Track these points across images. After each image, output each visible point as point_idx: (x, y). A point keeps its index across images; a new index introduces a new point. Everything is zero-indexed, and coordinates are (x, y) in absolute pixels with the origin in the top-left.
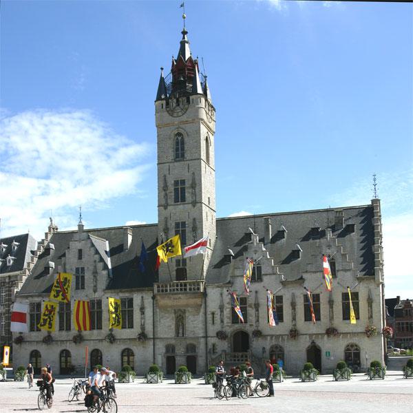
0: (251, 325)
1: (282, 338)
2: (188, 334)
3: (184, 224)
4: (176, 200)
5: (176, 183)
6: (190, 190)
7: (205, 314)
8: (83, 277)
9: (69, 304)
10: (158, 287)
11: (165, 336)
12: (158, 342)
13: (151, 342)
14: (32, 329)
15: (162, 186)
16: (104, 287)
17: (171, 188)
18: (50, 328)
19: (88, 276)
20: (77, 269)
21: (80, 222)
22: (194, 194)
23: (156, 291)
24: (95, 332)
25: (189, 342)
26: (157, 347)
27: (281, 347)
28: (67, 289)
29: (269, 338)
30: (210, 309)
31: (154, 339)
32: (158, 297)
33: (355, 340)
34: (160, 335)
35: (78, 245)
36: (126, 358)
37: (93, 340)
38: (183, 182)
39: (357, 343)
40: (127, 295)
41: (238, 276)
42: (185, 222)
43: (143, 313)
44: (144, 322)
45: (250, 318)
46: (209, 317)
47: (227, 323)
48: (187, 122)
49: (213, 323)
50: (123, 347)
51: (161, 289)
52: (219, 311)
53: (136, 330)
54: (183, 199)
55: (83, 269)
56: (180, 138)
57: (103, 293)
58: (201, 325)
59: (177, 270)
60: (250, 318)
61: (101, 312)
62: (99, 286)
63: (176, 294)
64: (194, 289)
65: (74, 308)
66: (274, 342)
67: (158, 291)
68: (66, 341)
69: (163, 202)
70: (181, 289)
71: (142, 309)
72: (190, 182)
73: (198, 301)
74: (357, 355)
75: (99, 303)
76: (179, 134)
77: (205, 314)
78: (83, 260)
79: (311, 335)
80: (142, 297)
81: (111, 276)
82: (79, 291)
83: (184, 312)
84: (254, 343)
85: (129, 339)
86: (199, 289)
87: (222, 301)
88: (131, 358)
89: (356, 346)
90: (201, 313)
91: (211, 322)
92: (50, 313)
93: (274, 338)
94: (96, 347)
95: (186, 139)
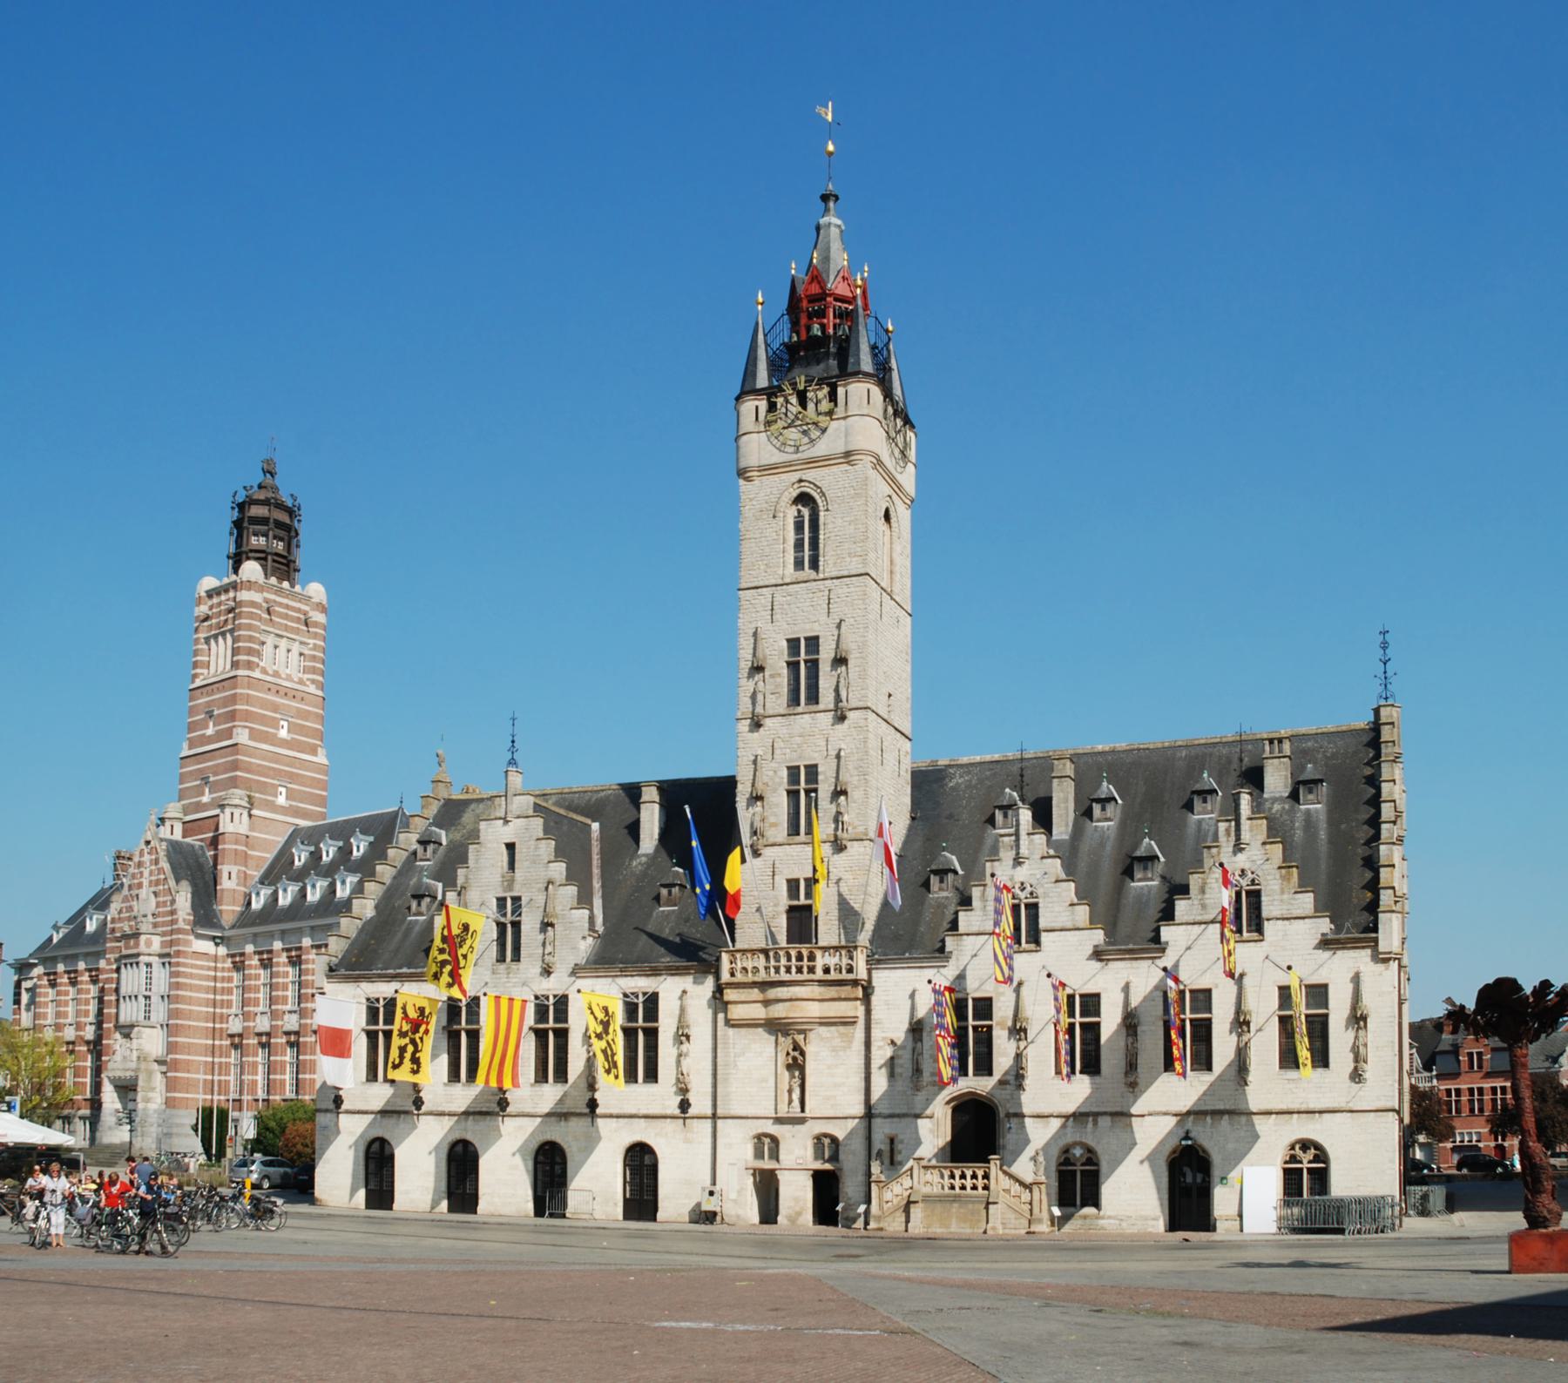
8: (516, 925)
13: (708, 1124)
18: (415, 1072)
19: (529, 924)
20: (501, 902)
28: (465, 957)
32: (730, 995)
40: (640, 984)
41: (968, 935)
42: (816, 766)
43: (682, 1036)
51: (739, 965)
55: (517, 900)
59: (792, 910)
70: (799, 970)
74: (1321, 1178)
75: (562, 1002)
78: (519, 873)
80: (684, 992)
81: (600, 927)
82: (502, 967)
84: (1009, 1136)
85: (646, 1117)
86: (850, 970)
89: (1318, 1147)
92: (415, 1029)
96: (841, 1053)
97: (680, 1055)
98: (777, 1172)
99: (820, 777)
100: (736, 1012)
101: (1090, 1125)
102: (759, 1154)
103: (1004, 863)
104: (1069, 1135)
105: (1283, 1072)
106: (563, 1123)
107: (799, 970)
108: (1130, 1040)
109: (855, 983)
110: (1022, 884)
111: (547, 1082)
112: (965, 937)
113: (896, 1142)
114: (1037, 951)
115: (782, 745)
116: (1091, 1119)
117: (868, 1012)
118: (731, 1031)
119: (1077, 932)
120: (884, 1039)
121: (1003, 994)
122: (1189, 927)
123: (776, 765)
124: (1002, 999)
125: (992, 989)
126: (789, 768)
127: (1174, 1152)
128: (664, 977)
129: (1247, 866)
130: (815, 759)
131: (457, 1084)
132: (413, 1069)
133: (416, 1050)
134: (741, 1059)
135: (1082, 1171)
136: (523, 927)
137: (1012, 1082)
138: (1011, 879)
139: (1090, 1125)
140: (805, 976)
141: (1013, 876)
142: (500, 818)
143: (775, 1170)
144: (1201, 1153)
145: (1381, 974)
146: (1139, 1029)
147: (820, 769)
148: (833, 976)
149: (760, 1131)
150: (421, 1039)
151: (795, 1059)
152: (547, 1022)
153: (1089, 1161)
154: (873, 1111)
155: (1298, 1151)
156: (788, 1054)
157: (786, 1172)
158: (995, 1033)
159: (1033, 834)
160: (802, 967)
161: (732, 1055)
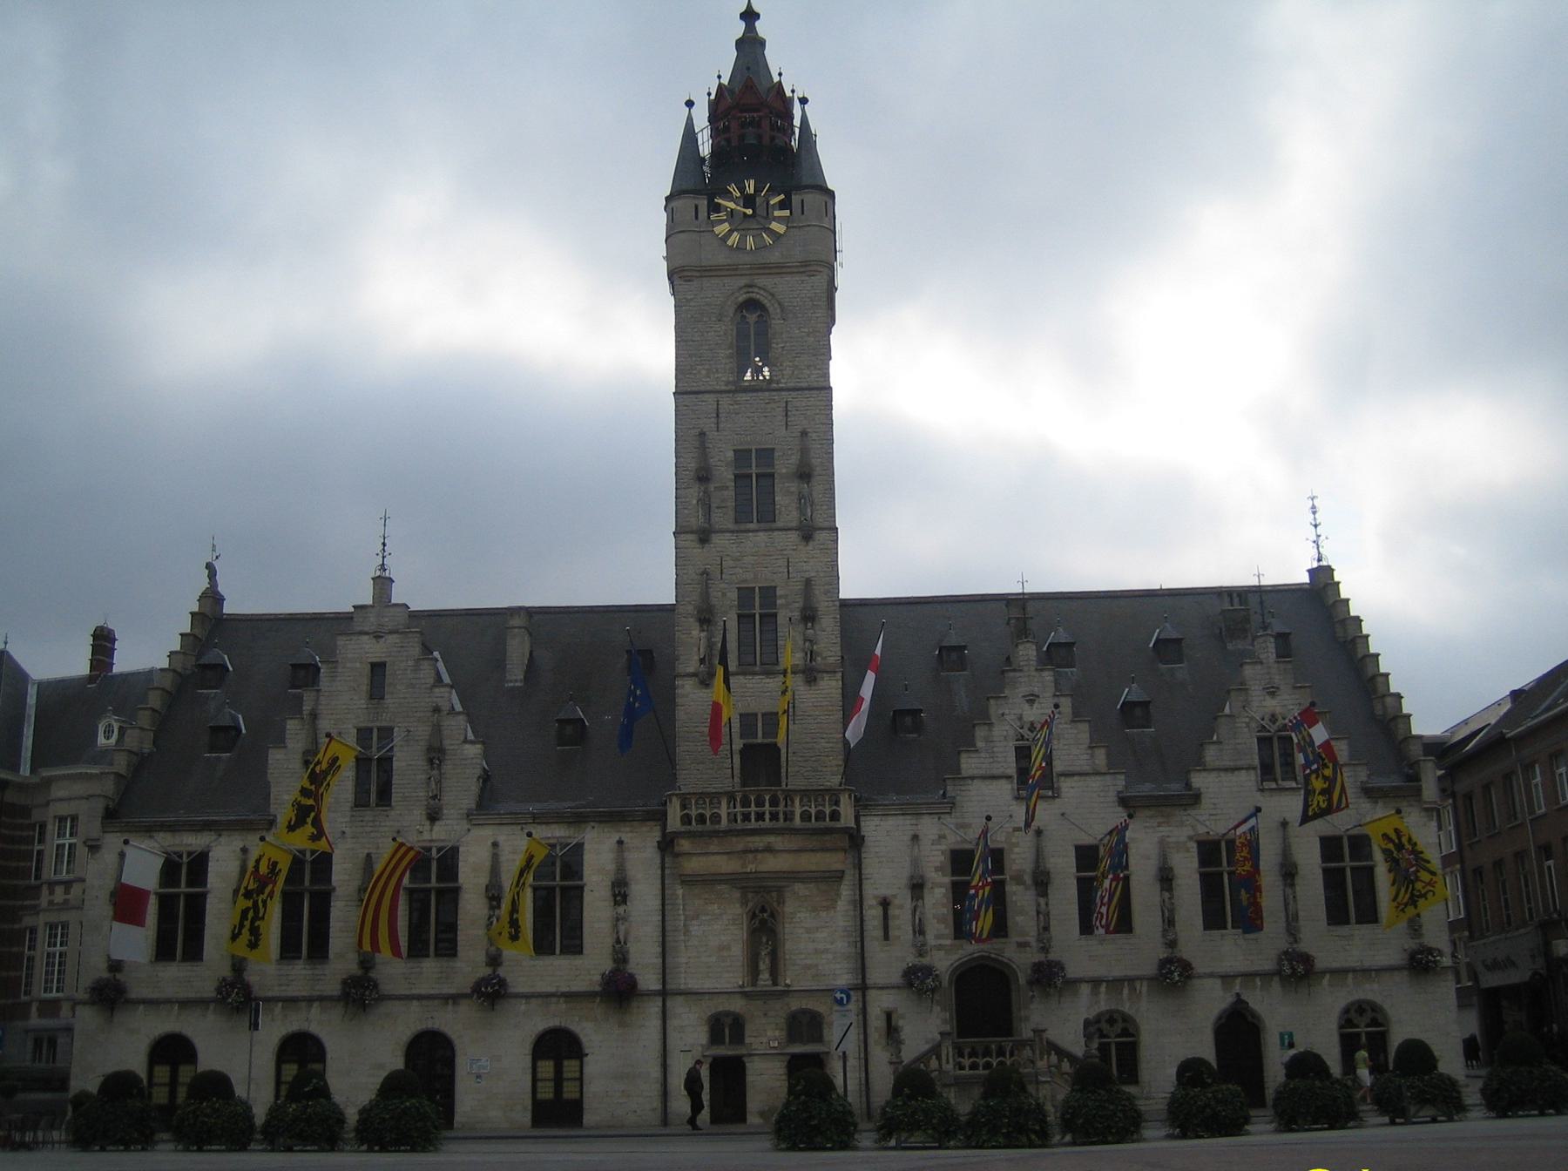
0: (1023, 945)
1: (1133, 989)
2: (792, 978)
3: (769, 593)
4: (742, 515)
5: (742, 456)
6: (794, 486)
7: (859, 903)
8: (386, 763)
9: (323, 863)
10: (684, 807)
11: (708, 985)
12: (677, 1006)
13: (654, 1007)
14: (164, 951)
15: (693, 465)
16: (469, 801)
17: (725, 474)
19: (407, 762)
20: (364, 734)
21: (383, 567)
22: (804, 501)
23: (674, 821)
24: (430, 966)
25: (795, 1004)
26: (673, 1023)
27: (1126, 1019)
29: (1085, 989)
30: (872, 892)
31: (664, 994)
32: (685, 845)
33: (1370, 991)
34: (687, 979)
35: (374, 650)
36: (546, 1068)
37: (420, 998)
38: (766, 455)
39: (1378, 1000)
40: (558, 832)
41: (972, 778)
44: (627, 934)
45: (1019, 919)
46: (873, 914)
47: (938, 937)
48: (779, 269)
49: (886, 937)
50: (541, 1023)
51: (694, 813)
52: (907, 894)
53: (591, 966)
54: (767, 516)
55: (386, 733)
56: (752, 318)
57: (465, 825)
58: (842, 946)
59: (747, 751)
60: (1019, 919)
61: (456, 891)
62: (447, 798)
63: (754, 832)
64: (820, 816)
65: (343, 875)
66: (1104, 1004)
67: (686, 820)
68: (310, 1000)
69: (697, 521)
70: (760, 817)
71: (620, 892)
72: (794, 459)
73: (834, 861)
75: (449, 861)
76: (751, 305)
77: (859, 903)
79: (1227, 979)
80: (620, 842)
82: (368, 815)
83: (781, 901)
86: (835, 816)
87: (915, 862)
88: (570, 1066)
89: (1375, 1008)
90: (843, 905)
91: (879, 933)
92: (260, 891)
93: (1103, 988)
94: (430, 1025)
95: (776, 323)
96: (823, 914)
97: (618, 920)
98: (745, 1059)
99: (779, 602)
100: (693, 865)
101: (1126, 991)
102: (716, 1036)
103: (1011, 701)
104: (1102, 1003)
105: (1331, 928)
106: (450, 1007)
107: (760, 817)
108: (1167, 895)
109: (846, 830)
110: (1032, 723)
111: (428, 956)
112: (970, 782)
113: (894, 1017)
114: (1053, 797)
115: (731, 563)
116: (1126, 984)
117: (859, 866)
118: (680, 892)
119: (1098, 778)
120: (875, 897)
121: (1017, 845)
122: (1222, 774)
123: (726, 586)
124: (1016, 850)
125: (1003, 839)
126: (739, 589)
127: (1220, 1018)
128: (592, 824)
129: (1278, 710)
130: (773, 581)
131: (297, 962)
132: (250, 941)
133: (256, 917)
134: (694, 922)
135: (1117, 1044)
136: (395, 764)
137: (1034, 943)
138: (1020, 718)
139: (1126, 991)
140: (781, 823)
141: (1021, 715)
142: (366, 633)
143: (744, 1055)
144: (1250, 1019)
145: (1425, 825)
146: (1174, 882)
147: (779, 592)
148: (814, 823)
149: (721, 1009)
150: (264, 902)
151: (763, 922)
152: (429, 882)
153: (1125, 1032)
154: (868, 982)
155: (1353, 1015)
156: (754, 916)
157: (756, 1058)
158: (1011, 888)
159: (1042, 670)
160: (777, 813)
161: (682, 917)
